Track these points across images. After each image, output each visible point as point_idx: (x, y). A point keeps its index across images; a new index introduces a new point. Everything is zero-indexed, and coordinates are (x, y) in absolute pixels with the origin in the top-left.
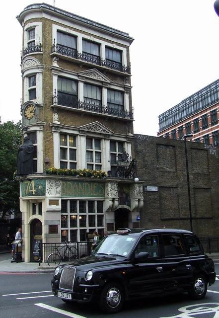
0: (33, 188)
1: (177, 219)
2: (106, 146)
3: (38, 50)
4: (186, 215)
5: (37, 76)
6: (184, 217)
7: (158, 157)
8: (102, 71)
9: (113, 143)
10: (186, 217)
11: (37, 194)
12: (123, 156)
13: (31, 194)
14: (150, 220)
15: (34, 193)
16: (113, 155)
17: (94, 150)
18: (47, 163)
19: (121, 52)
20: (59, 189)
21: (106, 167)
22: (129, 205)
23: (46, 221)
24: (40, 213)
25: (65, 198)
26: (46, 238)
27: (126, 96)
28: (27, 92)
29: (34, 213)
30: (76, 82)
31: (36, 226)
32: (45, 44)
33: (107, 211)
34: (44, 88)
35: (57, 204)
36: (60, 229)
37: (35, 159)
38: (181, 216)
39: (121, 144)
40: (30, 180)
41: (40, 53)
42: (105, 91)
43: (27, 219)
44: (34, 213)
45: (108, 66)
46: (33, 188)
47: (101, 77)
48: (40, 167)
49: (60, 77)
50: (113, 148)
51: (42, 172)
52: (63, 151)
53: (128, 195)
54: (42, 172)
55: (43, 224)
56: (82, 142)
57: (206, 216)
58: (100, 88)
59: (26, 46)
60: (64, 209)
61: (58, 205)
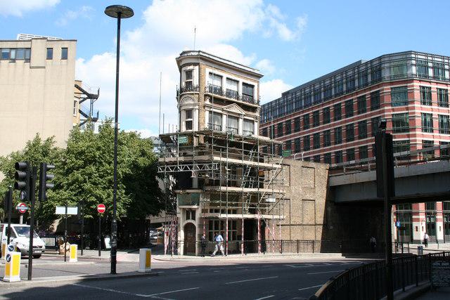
8: (239, 104)
19: (253, 86)
24: (194, 218)
28: (184, 124)
29: (188, 218)
30: (221, 115)
42: (241, 121)
43: (182, 223)
44: (188, 218)
45: (244, 101)
47: (236, 109)
49: (210, 112)
55: (197, 227)
57: (310, 223)
58: (238, 119)
59: (184, 84)
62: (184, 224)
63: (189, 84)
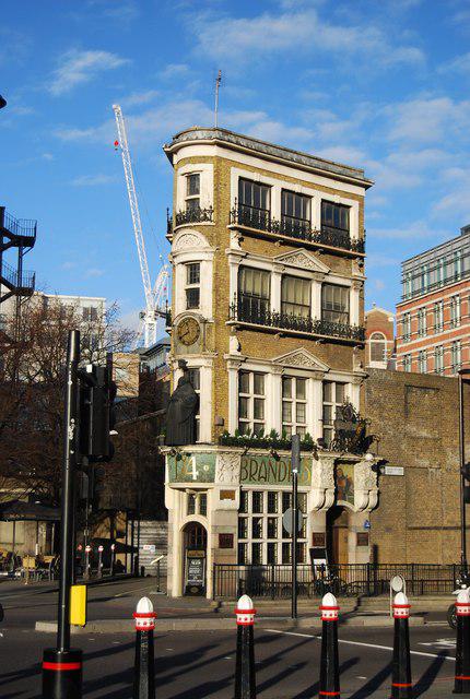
0: (194, 469)
1: (436, 528)
2: (313, 390)
3: (205, 219)
4: (453, 522)
5: (202, 265)
6: (449, 525)
7: (407, 412)
9: (326, 383)
10: (454, 525)
11: (200, 480)
12: (346, 411)
13: (189, 480)
14: (388, 529)
15: (195, 478)
16: (326, 409)
17: (294, 398)
18: (220, 424)
20: (237, 471)
21: (315, 431)
22: (352, 502)
23: (215, 527)
24: (203, 511)
25: (245, 487)
26: (215, 556)
27: (354, 296)
31: (194, 535)
32: (218, 208)
33: (314, 512)
34: (216, 290)
35: (233, 498)
36: (236, 541)
37: (197, 417)
38: (446, 524)
39: (341, 384)
40: (189, 455)
41: (209, 223)
44: (191, 510)
46: (194, 469)
48: (206, 431)
50: (326, 397)
51: (209, 440)
52: (242, 402)
53: (350, 483)
54: (209, 440)
56: (272, 385)
60: (242, 509)
61: (233, 498)
62: (182, 525)
63: (193, 203)
